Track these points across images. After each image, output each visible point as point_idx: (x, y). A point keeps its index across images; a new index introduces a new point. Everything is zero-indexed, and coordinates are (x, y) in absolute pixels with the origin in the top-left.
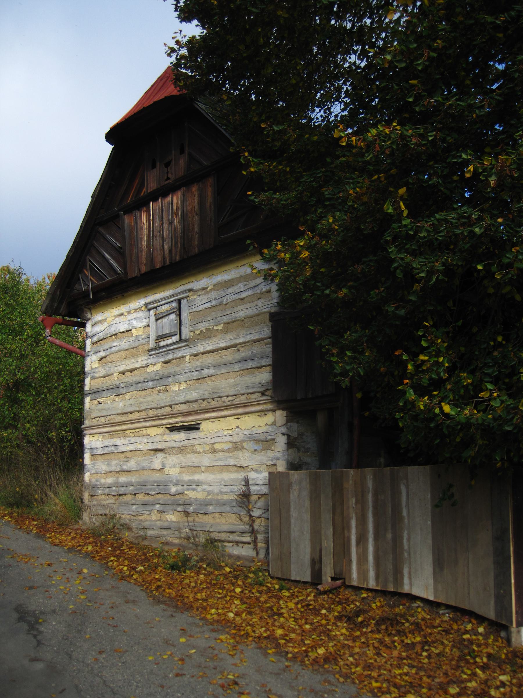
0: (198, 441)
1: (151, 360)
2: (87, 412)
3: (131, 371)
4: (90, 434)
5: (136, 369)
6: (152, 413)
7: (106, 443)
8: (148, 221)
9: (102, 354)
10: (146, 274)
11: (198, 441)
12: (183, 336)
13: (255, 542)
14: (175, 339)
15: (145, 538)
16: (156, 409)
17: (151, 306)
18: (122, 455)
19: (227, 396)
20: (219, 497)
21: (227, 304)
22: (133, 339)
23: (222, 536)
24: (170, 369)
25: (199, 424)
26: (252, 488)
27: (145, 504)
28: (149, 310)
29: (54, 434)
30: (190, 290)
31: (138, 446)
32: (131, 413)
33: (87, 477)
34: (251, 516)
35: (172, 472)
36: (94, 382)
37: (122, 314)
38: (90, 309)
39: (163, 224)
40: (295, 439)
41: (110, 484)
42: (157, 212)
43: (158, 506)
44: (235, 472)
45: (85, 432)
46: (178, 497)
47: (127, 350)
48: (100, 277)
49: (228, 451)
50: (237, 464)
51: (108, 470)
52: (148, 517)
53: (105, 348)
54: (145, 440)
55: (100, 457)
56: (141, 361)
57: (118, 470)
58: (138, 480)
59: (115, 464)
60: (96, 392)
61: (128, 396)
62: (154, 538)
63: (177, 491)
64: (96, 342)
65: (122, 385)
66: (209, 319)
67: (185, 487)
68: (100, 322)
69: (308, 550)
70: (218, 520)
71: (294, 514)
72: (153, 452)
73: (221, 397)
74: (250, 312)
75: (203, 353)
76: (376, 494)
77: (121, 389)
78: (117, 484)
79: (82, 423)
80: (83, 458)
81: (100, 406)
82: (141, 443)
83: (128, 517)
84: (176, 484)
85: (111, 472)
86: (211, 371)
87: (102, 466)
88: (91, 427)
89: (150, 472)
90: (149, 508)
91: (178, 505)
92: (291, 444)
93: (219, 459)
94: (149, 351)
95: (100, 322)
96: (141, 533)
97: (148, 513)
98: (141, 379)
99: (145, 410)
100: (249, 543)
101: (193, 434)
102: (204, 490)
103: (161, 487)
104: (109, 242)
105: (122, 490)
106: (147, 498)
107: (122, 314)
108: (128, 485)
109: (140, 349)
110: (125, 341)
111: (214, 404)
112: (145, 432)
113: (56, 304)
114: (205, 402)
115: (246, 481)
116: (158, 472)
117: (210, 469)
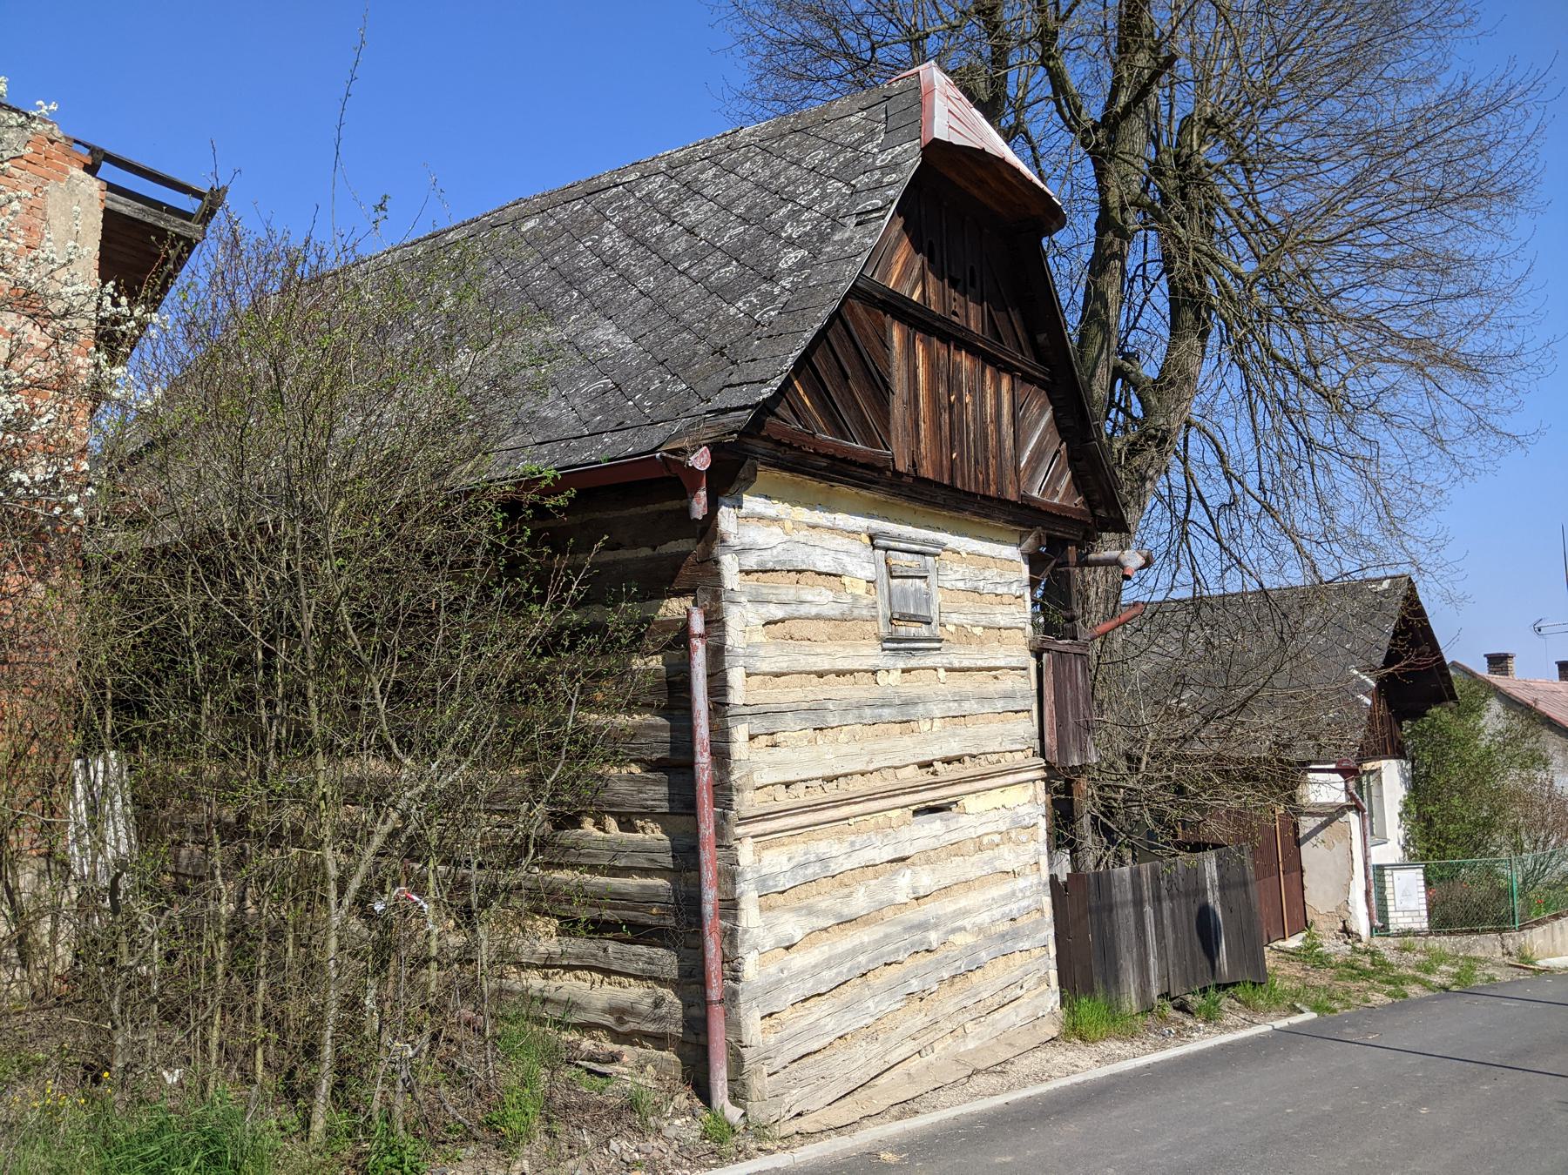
3: (839, 673)
4: (753, 837)
9: (777, 612)
17: (882, 542)
30: (942, 545)
44: (996, 884)
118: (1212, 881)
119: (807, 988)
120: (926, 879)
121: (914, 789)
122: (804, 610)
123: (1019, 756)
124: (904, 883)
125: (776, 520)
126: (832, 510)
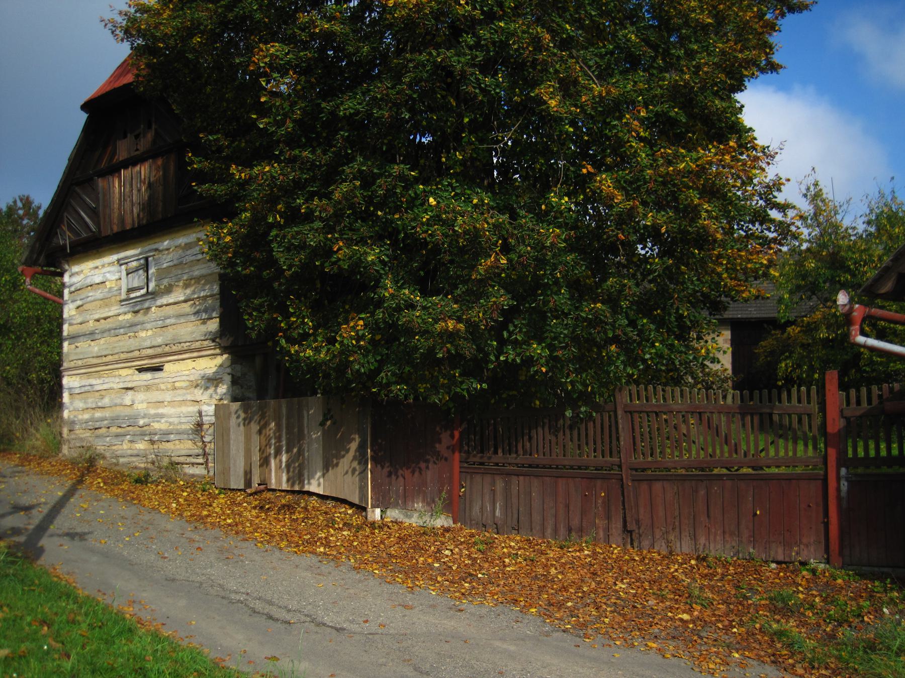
0: (161, 380)
1: (123, 309)
2: (66, 355)
3: (105, 319)
5: (109, 317)
6: (123, 356)
7: (83, 384)
8: (120, 186)
9: (79, 303)
10: (117, 233)
11: (161, 380)
12: (150, 289)
13: (207, 462)
14: (143, 291)
15: (117, 464)
16: (127, 352)
17: (122, 262)
18: (97, 394)
19: (185, 342)
20: (179, 427)
21: (186, 264)
22: (107, 290)
23: (182, 459)
24: (140, 317)
25: (163, 366)
26: (205, 419)
27: (117, 436)
28: (121, 265)
29: (34, 376)
30: (156, 250)
31: (112, 385)
32: (105, 356)
33: (66, 414)
34: (203, 442)
35: (140, 407)
36: (71, 328)
37: (97, 267)
38: (68, 262)
39: (132, 190)
40: (239, 378)
41: (87, 419)
42: (129, 178)
43: (128, 437)
44: (191, 406)
45: (64, 373)
46: (145, 428)
47: (102, 300)
48: (77, 234)
49: (186, 388)
50: (193, 399)
51: (85, 407)
52: (120, 447)
53: (82, 297)
54: (117, 380)
55: (77, 396)
56: (114, 310)
57: (94, 406)
58: (111, 415)
59: (91, 403)
60: (73, 338)
61: (102, 341)
62: (123, 465)
63: (144, 423)
64: (74, 292)
65: (97, 331)
66: (172, 275)
67: (151, 420)
68: (77, 273)
69: (242, 464)
70: (178, 447)
71: (232, 436)
72: (124, 390)
73: (180, 343)
74: (204, 271)
75: (166, 305)
76: (288, 419)
77: (96, 335)
78: (92, 419)
79: (61, 365)
80: (61, 397)
81: (78, 350)
82: (113, 382)
83: (103, 447)
84: (143, 418)
85: (87, 409)
86: (173, 321)
87: (80, 404)
88: (69, 369)
89: (122, 408)
90: (121, 439)
91: (145, 435)
92: (235, 382)
93: (179, 395)
94: (121, 301)
95: (77, 273)
96: (114, 461)
97: (120, 443)
98: (114, 326)
99: (117, 353)
100: (202, 464)
101: (158, 374)
102: (166, 422)
103: (131, 420)
104: (84, 201)
105: (98, 425)
106: (119, 430)
107: (97, 267)
108: (102, 419)
109: (113, 299)
110: (100, 291)
111: (175, 348)
112: (117, 373)
113: (35, 256)
114: (168, 347)
115: (200, 413)
116: (128, 408)
117: (171, 403)
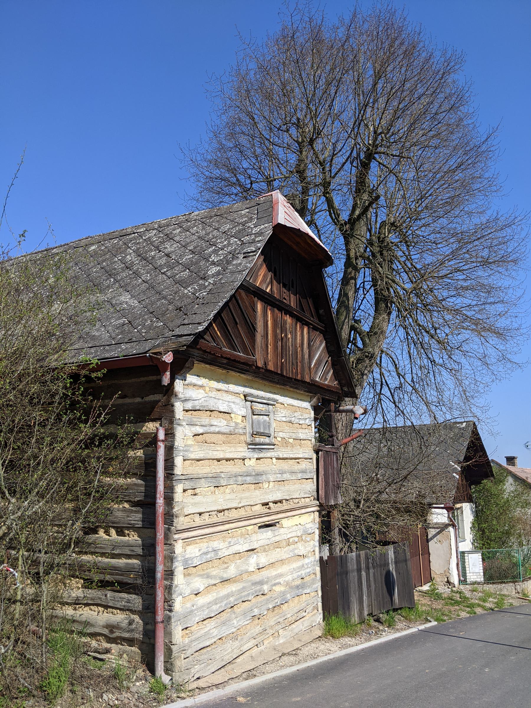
3: (227, 460)
4: (182, 539)
9: (200, 430)
17: (249, 398)
30: (276, 401)
118: (392, 560)
119: (205, 614)
120: (263, 559)
121: (260, 516)
122: (212, 429)
123: (307, 500)
124: (253, 561)
125: (202, 387)
126: (228, 383)
